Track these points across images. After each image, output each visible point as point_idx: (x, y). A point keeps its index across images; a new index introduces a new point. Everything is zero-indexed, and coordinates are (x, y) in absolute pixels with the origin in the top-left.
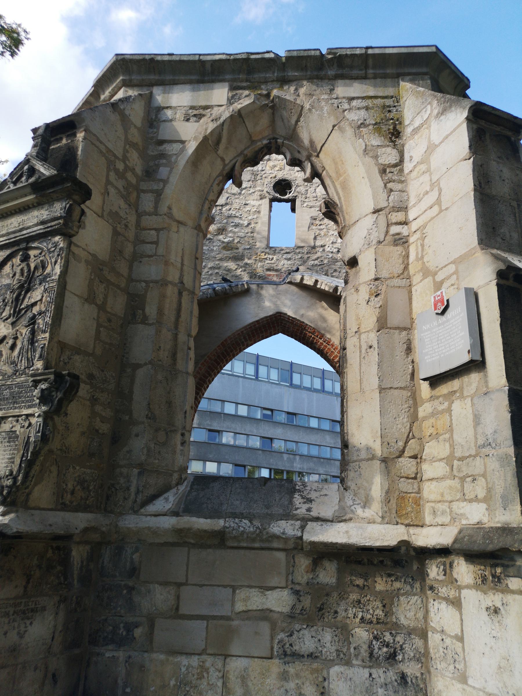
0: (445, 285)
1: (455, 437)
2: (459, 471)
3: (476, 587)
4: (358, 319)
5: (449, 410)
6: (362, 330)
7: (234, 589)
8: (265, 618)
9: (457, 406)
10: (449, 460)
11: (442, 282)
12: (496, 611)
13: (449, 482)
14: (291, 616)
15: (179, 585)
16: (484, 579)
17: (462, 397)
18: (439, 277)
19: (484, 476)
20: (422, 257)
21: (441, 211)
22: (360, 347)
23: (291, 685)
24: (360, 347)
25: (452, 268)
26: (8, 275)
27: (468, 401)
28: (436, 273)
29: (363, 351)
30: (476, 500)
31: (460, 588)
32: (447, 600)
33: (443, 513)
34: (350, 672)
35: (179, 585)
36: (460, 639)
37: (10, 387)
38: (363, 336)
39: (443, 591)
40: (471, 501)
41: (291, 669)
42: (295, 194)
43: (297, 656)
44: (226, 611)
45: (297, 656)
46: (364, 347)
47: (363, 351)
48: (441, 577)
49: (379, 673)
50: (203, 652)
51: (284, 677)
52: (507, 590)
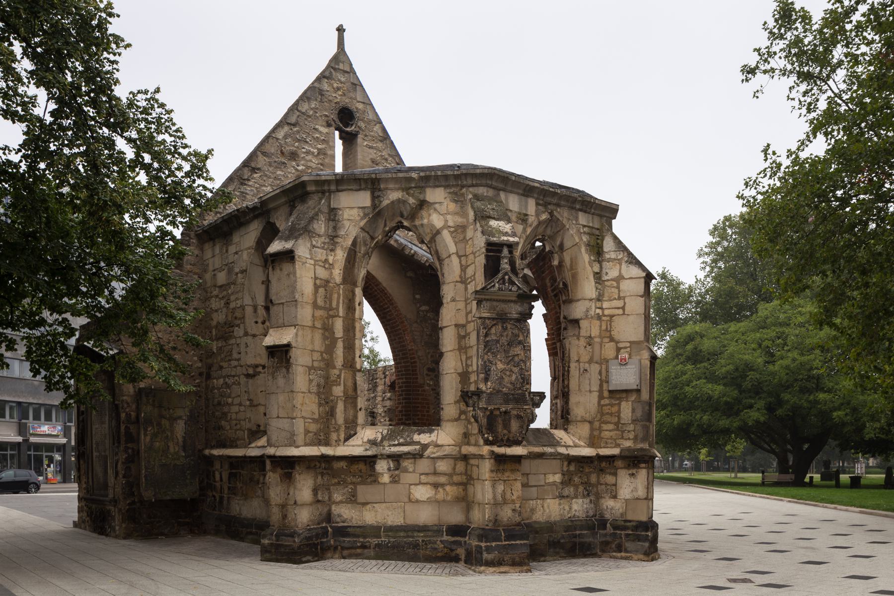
0: (622, 351)
1: (622, 415)
2: (622, 427)
3: (625, 468)
4: (578, 354)
5: (619, 404)
6: (581, 360)
7: (545, 474)
8: (555, 485)
9: (624, 404)
10: (617, 424)
11: (621, 348)
12: (633, 474)
13: (616, 432)
14: (562, 483)
15: (528, 474)
16: (629, 465)
17: (627, 401)
18: (621, 345)
19: (634, 431)
20: (610, 331)
21: (624, 314)
22: (579, 369)
23: (562, 507)
24: (579, 369)
25: (628, 345)
26: (496, 334)
27: (630, 403)
28: (618, 342)
29: (581, 371)
30: (629, 439)
31: (617, 469)
32: (610, 474)
33: (611, 443)
34: (577, 500)
35: (528, 474)
36: (615, 485)
37: (513, 394)
38: (581, 364)
39: (608, 471)
40: (626, 439)
41: (562, 502)
42: (357, 129)
43: (563, 497)
44: (542, 483)
45: (563, 497)
46: (582, 370)
47: (581, 371)
48: (608, 466)
49: (585, 500)
50: (537, 498)
51: (560, 504)
52: (639, 468)
